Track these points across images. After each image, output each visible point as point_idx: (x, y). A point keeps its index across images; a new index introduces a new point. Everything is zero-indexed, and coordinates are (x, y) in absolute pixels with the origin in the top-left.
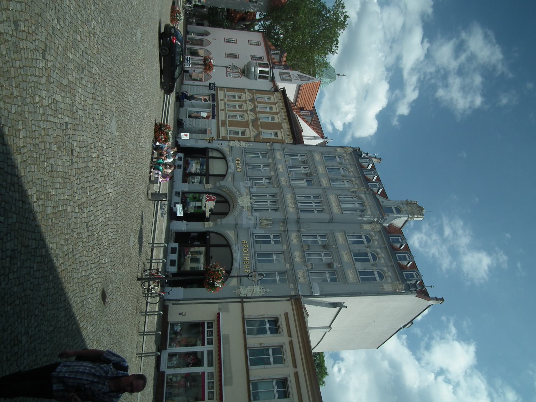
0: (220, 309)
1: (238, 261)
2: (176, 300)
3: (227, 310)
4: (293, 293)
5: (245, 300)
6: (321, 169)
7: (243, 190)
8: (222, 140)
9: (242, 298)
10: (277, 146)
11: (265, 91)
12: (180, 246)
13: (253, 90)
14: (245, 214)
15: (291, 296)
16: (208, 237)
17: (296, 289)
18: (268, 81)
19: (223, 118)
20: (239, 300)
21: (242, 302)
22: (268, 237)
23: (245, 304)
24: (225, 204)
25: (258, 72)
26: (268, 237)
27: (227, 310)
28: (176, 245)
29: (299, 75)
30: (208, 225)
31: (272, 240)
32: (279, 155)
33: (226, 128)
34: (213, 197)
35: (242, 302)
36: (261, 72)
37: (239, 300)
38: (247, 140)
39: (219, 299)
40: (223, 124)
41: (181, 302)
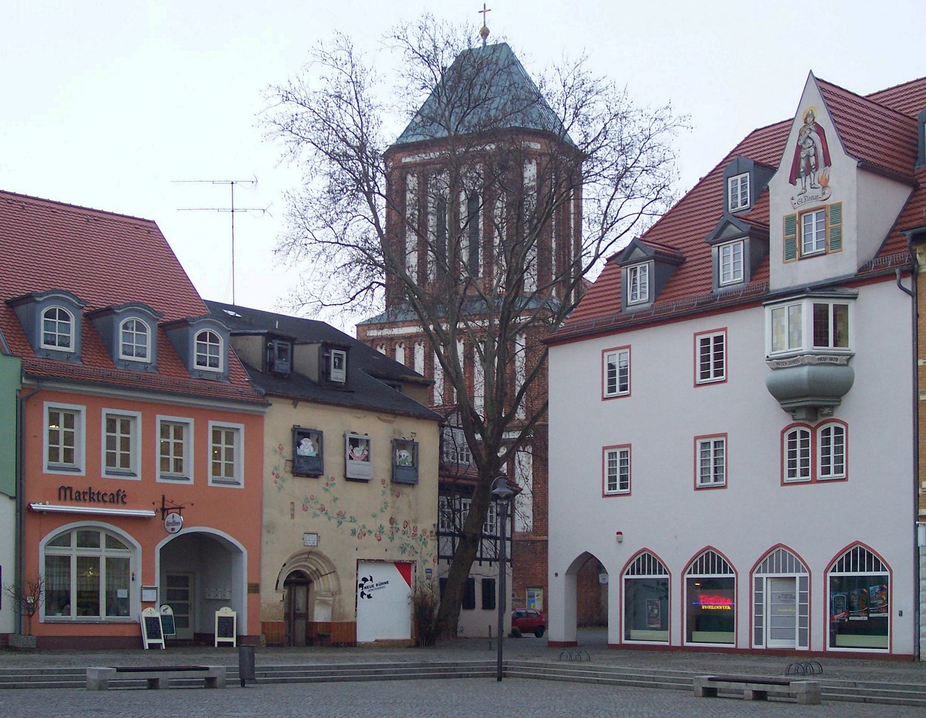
13: (916, 368)
18: (851, 305)
25: (822, 349)
36: (820, 337)
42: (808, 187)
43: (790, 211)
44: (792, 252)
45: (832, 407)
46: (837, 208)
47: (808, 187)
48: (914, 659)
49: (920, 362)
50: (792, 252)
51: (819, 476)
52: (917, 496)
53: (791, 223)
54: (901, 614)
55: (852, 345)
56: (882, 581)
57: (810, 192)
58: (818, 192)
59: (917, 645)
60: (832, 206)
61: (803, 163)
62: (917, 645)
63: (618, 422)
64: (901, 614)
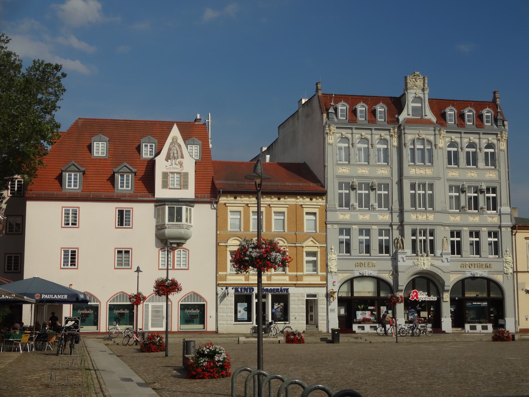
0: (522, 290)
1: (482, 273)
2: (515, 323)
3: (524, 284)
4: (509, 229)
5: (515, 270)
6: (364, 171)
7: (409, 263)
8: (327, 280)
9: (514, 272)
10: (331, 217)
11: (217, 217)
12: (469, 323)
14: (438, 263)
15: (512, 232)
16: (457, 299)
17: (506, 227)
18: (192, 208)
19: (287, 278)
20: (515, 274)
21: (517, 272)
22: (453, 242)
23: (518, 270)
24: (428, 281)
26: (453, 242)
27: (524, 284)
28: (467, 326)
29: (168, 158)
30: (446, 297)
31: (456, 239)
32: (345, 216)
33: (307, 275)
34: (413, 292)
35: (517, 272)
36: (187, 221)
37: (515, 274)
38: (325, 252)
39: (514, 290)
40: (297, 278)
41: (517, 320)
42: (174, 164)
43: (165, 171)
44: (165, 185)
45: (183, 243)
46: (186, 174)
47: (174, 164)
48: (216, 332)
49: (218, 232)
50: (165, 185)
51: (176, 267)
52: (217, 277)
53: (165, 175)
54: (211, 317)
55: (192, 224)
56: (203, 306)
57: (174, 166)
58: (179, 167)
59: (217, 328)
60: (184, 173)
61: (172, 155)
62: (217, 328)
63: (70, 238)
64: (211, 317)
